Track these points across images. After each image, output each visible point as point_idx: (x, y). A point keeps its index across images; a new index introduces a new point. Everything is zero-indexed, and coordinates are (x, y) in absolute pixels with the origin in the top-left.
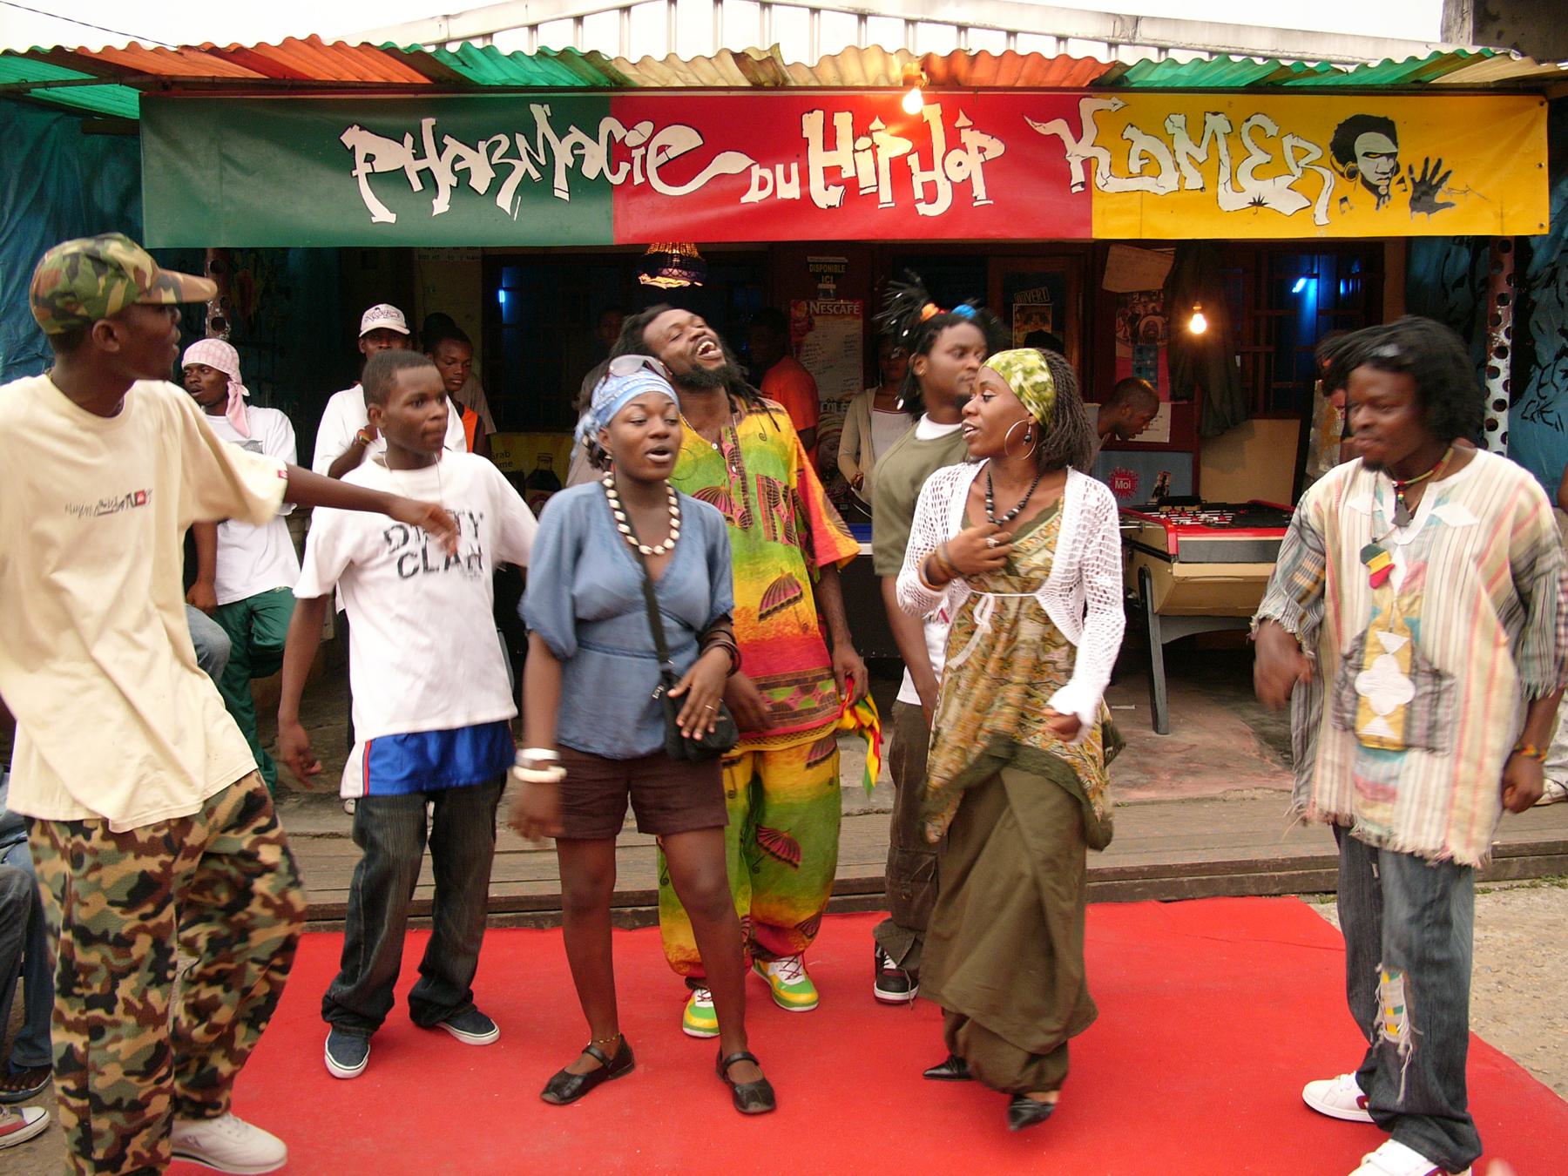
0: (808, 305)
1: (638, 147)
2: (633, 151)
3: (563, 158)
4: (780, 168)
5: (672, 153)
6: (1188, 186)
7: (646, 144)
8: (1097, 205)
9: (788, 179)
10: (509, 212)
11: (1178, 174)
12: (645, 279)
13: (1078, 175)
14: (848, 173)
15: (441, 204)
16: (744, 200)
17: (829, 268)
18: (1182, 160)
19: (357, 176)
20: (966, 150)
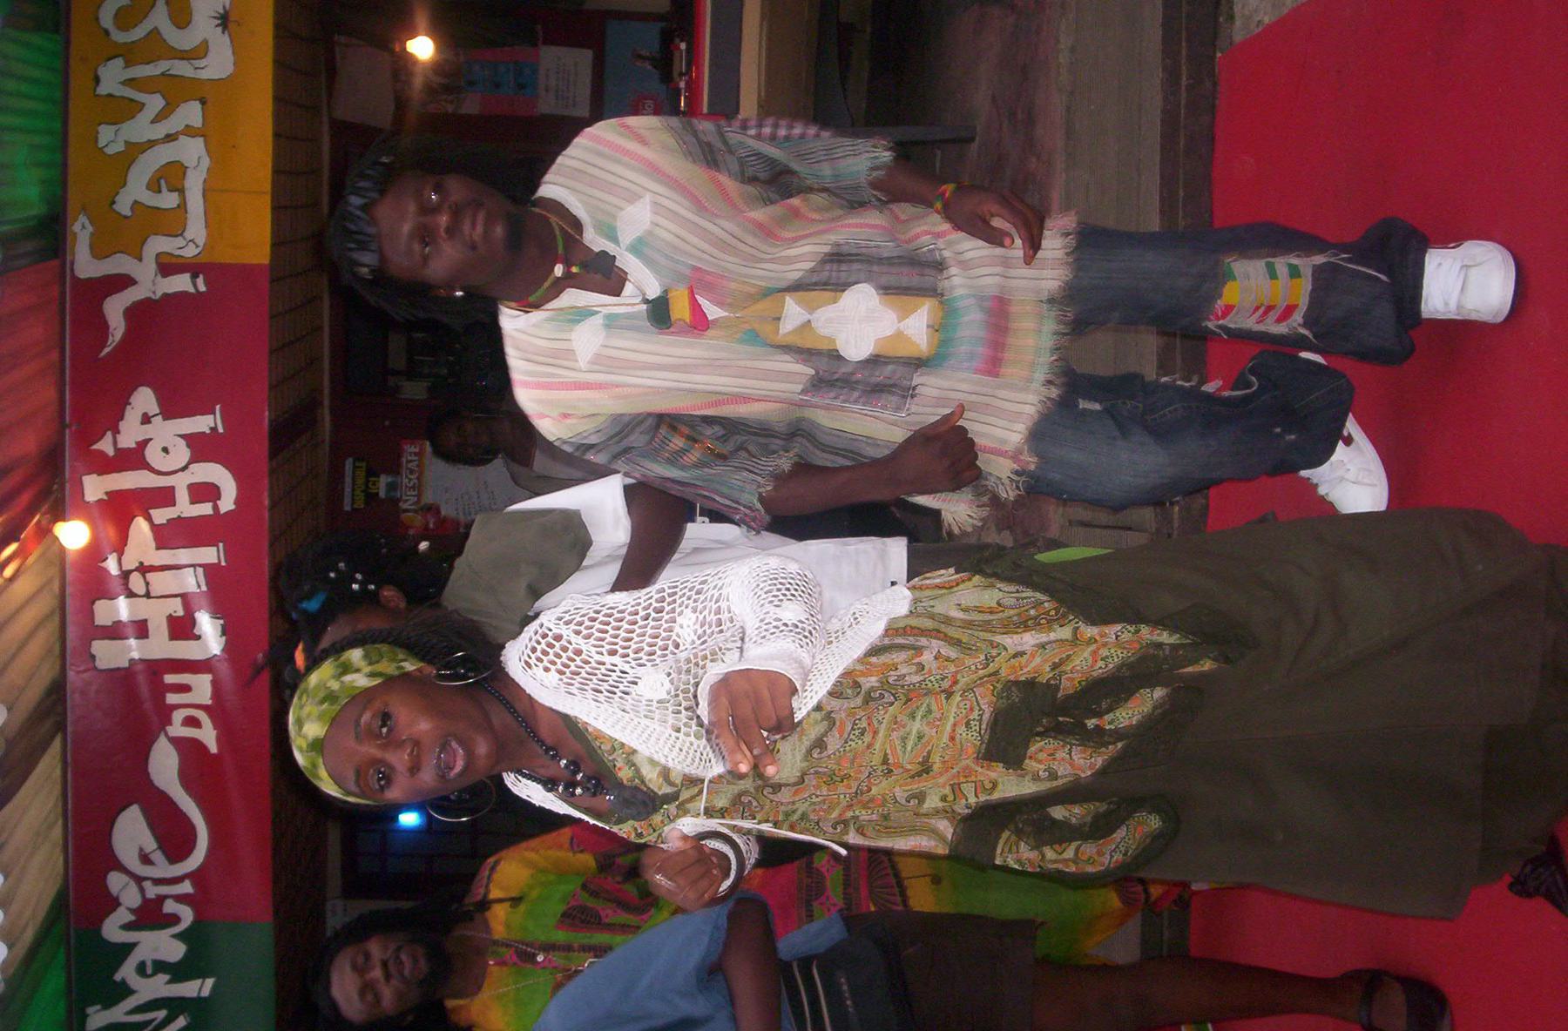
0: (407, 511)
1: (142, 890)
4: (172, 698)
5: (150, 844)
6: (197, 121)
7: (139, 880)
8: (226, 256)
9: (185, 688)
11: (182, 137)
13: (181, 283)
14: (177, 608)
16: (213, 749)
17: (360, 481)
18: (160, 131)
20: (145, 442)
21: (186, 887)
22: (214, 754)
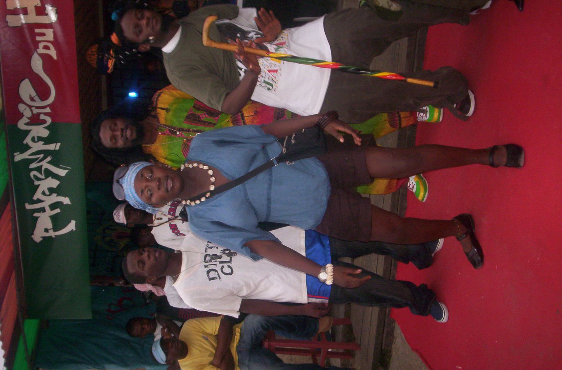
2: (34, 113)
3: (39, 146)
4: (38, 38)
5: (34, 94)
9: (43, 35)
10: (67, 171)
12: (109, 71)
15: (66, 201)
16: (55, 58)
19: (55, 236)
21: (48, 110)
22: (55, 60)
